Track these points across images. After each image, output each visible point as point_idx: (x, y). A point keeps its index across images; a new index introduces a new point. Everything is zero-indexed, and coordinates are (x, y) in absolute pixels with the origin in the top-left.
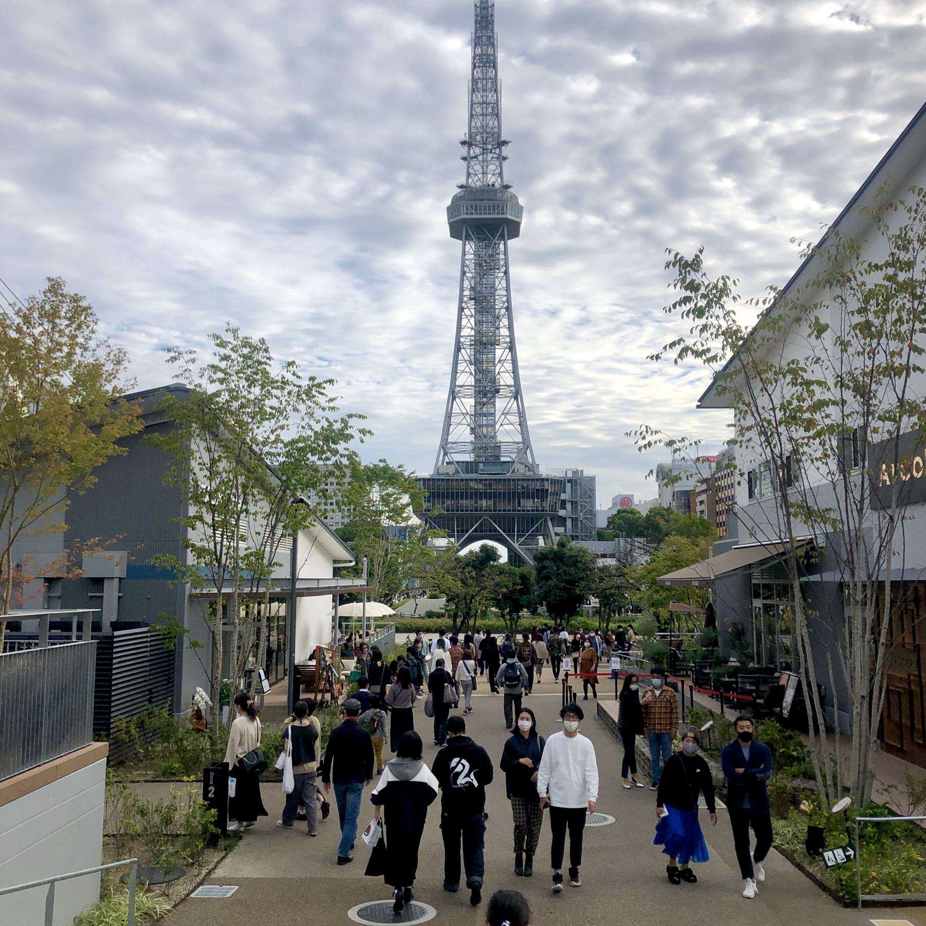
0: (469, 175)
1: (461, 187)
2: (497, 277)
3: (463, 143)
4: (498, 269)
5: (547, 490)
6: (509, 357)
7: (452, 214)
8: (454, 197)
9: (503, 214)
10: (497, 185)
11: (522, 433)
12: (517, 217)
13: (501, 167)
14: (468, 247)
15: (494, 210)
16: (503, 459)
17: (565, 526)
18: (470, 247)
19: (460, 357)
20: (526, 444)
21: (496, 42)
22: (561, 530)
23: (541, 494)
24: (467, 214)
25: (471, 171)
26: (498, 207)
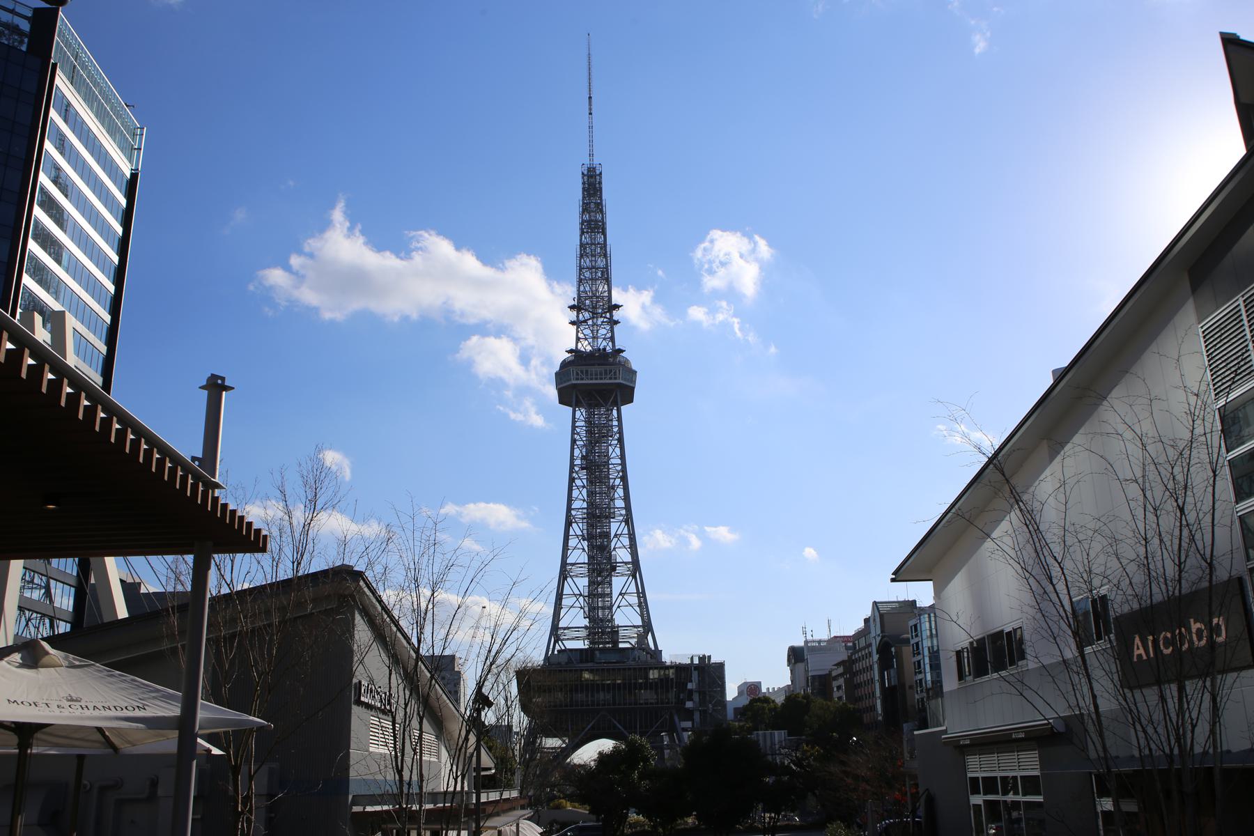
0: (578, 339)
1: (570, 351)
2: (610, 445)
3: (572, 307)
4: (611, 436)
6: (626, 531)
7: (561, 379)
8: (561, 364)
9: (615, 379)
10: (609, 349)
11: (642, 616)
13: (612, 331)
14: (578, 414)
15: (606, 374)
16: (621, 645)
17: (693, 720)
18: (581, 414)
19: (571, 532)
20: (647, 627)
21: (604, 208)
22: (688, 724)
24: (577, 379)
26: (611, 371)
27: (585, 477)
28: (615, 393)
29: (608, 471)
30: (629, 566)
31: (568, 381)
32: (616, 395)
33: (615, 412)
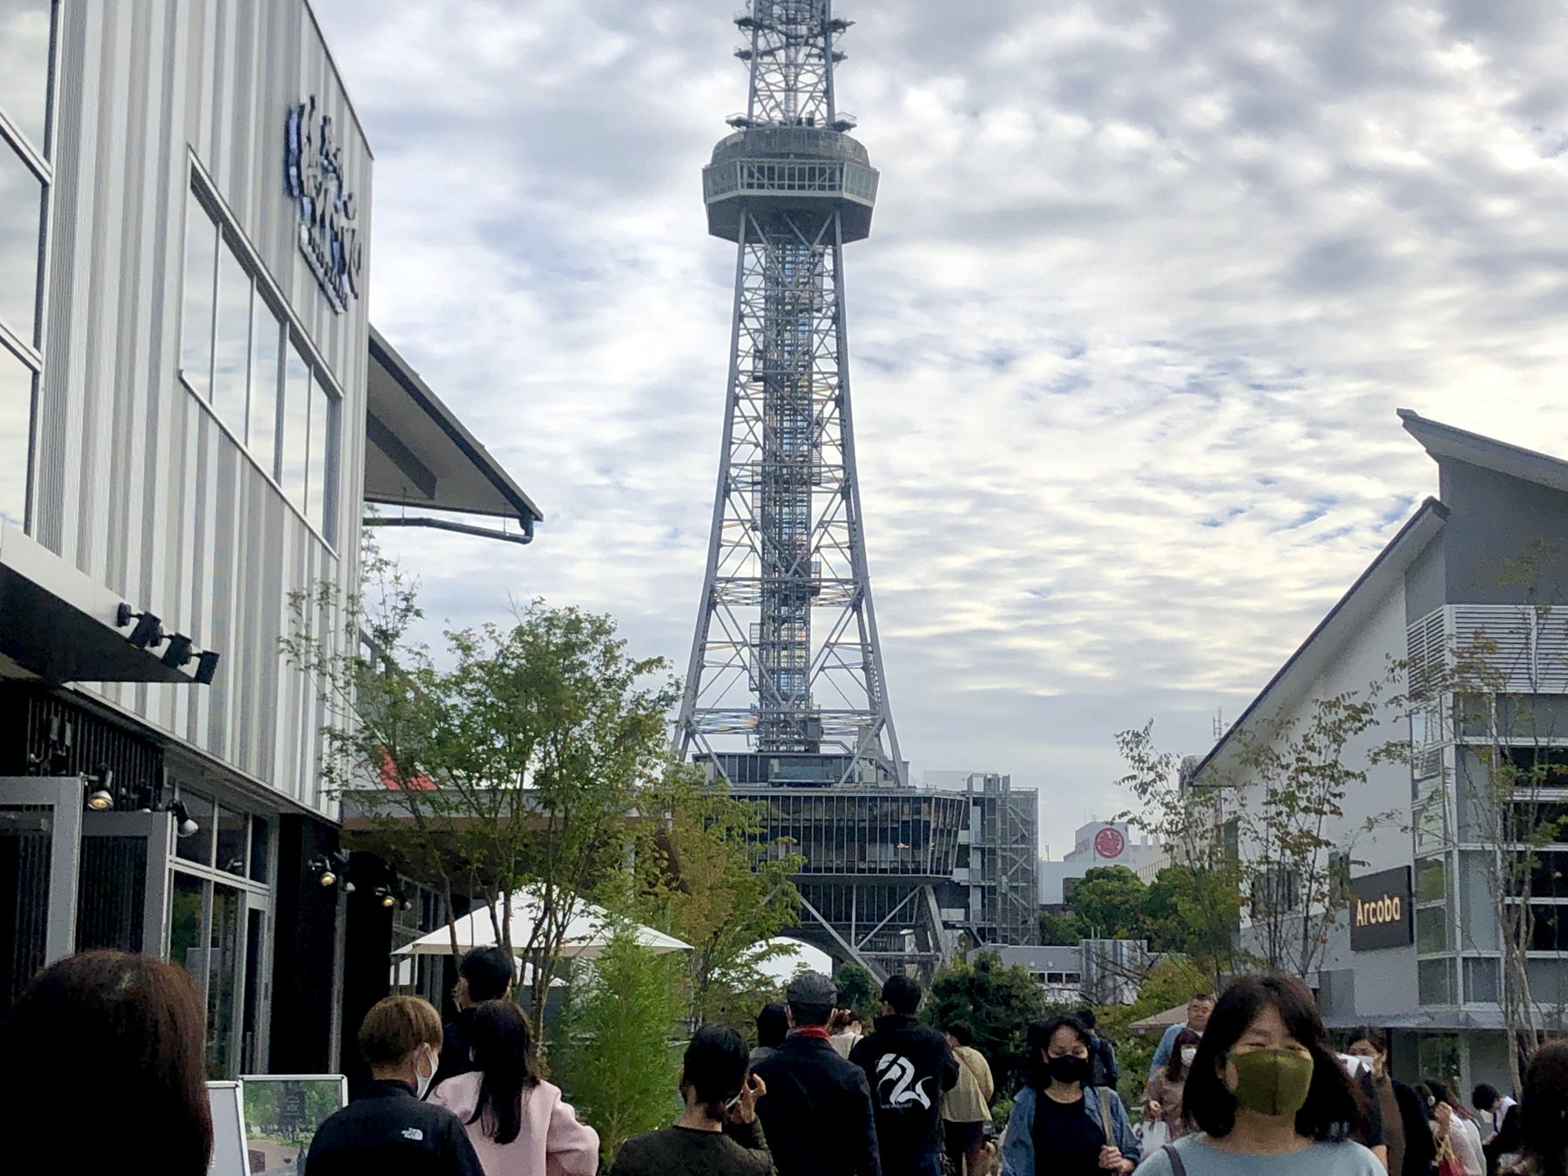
1: (738, 123)
2: (817, 332)
3: (743, 23)
4: (819, 310)
5: (927, 824)
6: (842, 515)
7: (715, 183)
8: (717, 147)
9: (832, 188)
10: (820, 123)
11: (870, 689)
12: (866, 196)
13: (828, 76)
14: (750, 260)
15: (812, 177)
16: (825, 750)
17: (967, 907)
18: (756, 257)
19: (729, 513)
20: (878, 715)
22: (956, 915)
23: (915, 834)
24: (750, 186)
25: (760, 85)
26: (822, 171)
27: (762, 395)
28: (829, 221)
29: (810, 386)
30: (847, 587)
31: (730, 189)
32: (833, 222)
33: (828, 263)
